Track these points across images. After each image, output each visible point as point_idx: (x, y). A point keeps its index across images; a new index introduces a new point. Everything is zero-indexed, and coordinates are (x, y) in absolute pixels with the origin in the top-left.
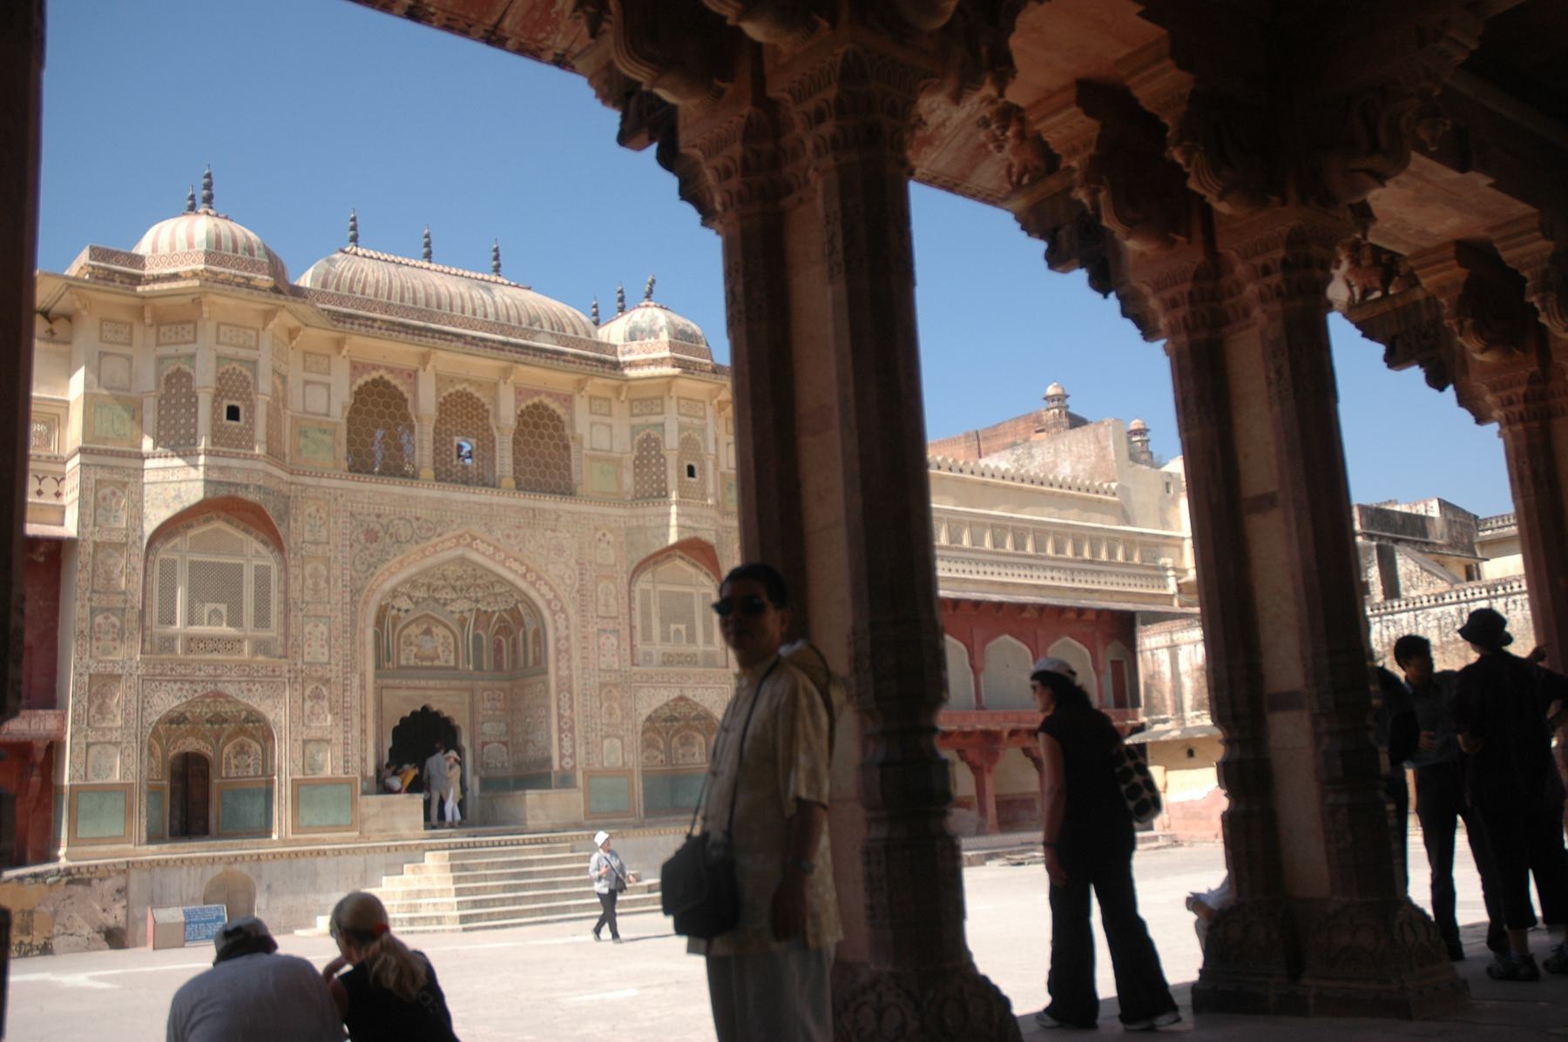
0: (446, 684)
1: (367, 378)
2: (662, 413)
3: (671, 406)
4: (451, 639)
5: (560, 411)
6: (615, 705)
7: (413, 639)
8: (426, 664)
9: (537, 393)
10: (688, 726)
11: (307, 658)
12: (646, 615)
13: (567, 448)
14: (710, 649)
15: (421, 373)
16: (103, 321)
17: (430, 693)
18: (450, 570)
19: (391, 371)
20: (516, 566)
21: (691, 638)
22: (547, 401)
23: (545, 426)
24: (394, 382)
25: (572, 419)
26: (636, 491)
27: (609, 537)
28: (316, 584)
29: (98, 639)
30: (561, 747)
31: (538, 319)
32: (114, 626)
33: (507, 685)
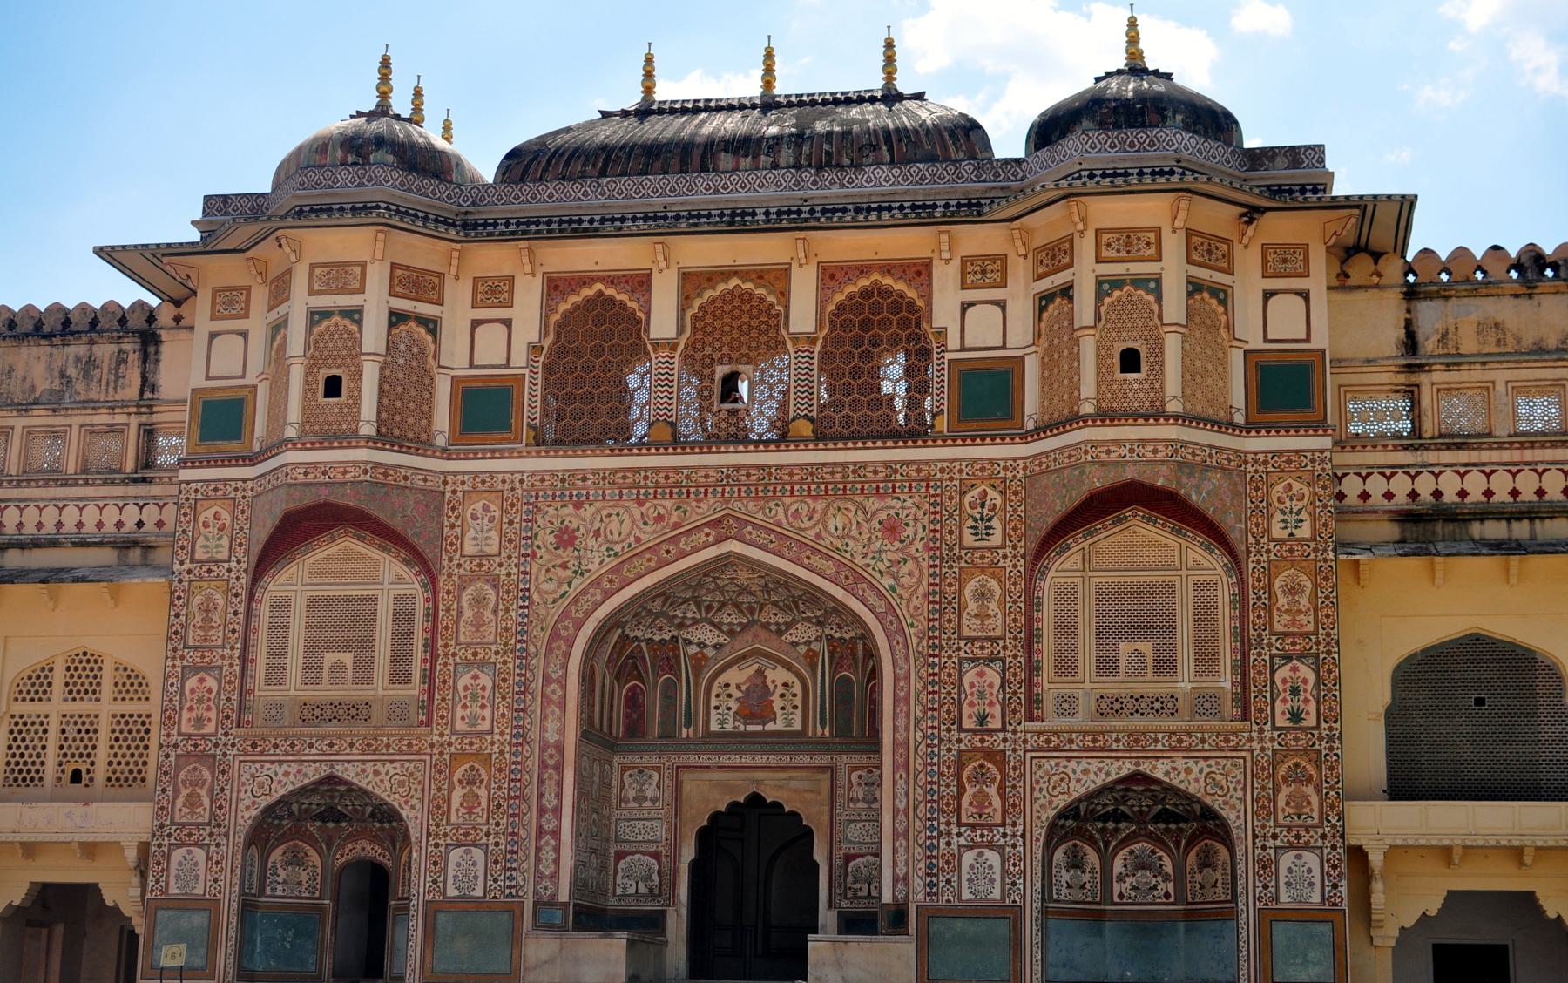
0: (785, 759)
1: (573, 299)
2: (1070, 265)
3: (1086, 248)
4: (798, 689)
5: (911, 294)
6: (992, 791)
8: (750, 728)
9: (863, 269)
10: (1203, 832)
11: (460, 726)
12: (1066, 628)
13: (925, 354)
14: (1207, 682)
15: (656, 277)
16: (216, 292)
17: (759, 775)
18: (743, 576)
19: (611, 279)
20: (817, 561)
21: (1166, 664)
22: (887, 281)
23: (884, 323)
24: (618, 297)
25: (929, 303)
26: (1043, 410)
28: (478, 616)
29: (191, 709)
30: (895, 864)
31: (875, 147)
32: (210, 691)
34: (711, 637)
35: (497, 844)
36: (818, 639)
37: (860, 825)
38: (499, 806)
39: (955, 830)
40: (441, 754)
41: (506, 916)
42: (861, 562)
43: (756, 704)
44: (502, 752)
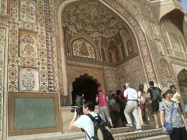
4: (93, 49)
6: (167, 69)
7: (78, 46)
8: (84, 56)
17: (86, 69)
20: (120, 9)
27: (149, 8)
33: (115, 68)
34: (74, 31)
35: (43, 68)
36: (99, 37)
37: (111, 83)
38: (43, 53)
39: (165, 78)
40: (14, 27)
41: (51, 100)
42: (131, 12)
43: (84, 52)
44: (42, 33)
